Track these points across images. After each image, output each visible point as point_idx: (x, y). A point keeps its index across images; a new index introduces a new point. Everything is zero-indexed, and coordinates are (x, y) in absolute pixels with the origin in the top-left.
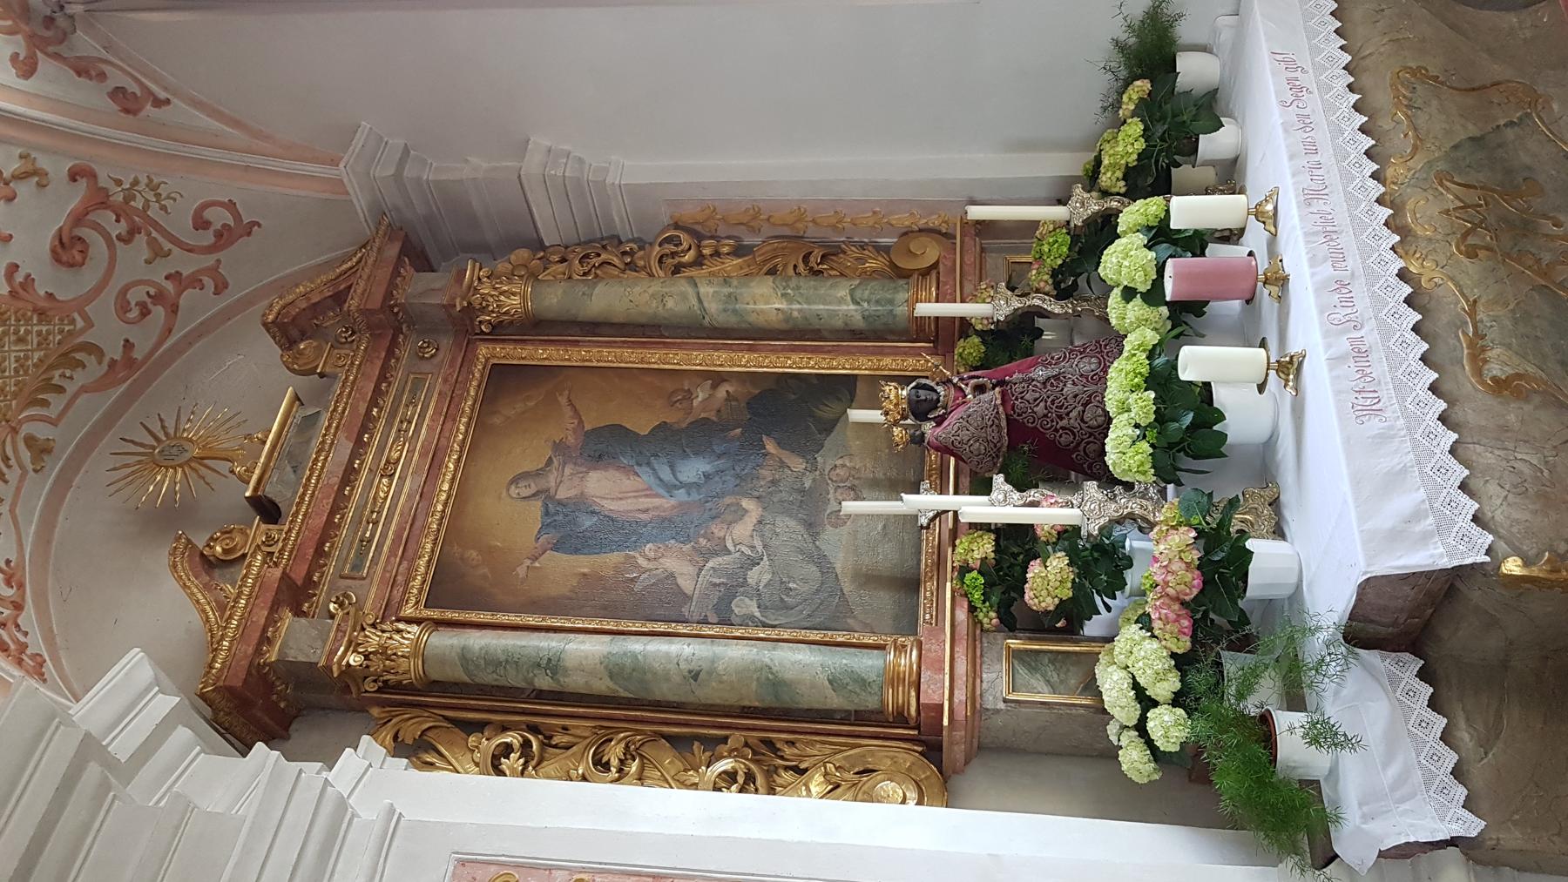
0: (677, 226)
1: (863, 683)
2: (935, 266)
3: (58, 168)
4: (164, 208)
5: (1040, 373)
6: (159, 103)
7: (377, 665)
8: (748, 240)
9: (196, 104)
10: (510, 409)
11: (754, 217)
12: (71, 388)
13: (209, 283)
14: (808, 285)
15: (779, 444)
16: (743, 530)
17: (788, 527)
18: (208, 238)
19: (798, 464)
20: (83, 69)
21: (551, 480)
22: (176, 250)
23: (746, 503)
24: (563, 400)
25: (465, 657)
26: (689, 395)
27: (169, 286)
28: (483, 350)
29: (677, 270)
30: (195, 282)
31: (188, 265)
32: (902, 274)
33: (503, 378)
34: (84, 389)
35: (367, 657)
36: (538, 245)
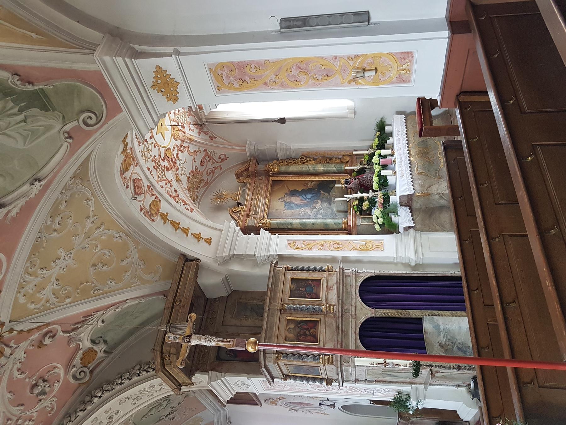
0: (303, 155)
1: (339, 224)
2: (348, 161)
3: (202, 149)
4: (215, 155)
5: (364, 176)
6: (215, 138)
7: (263, 225)
8: (315, 158)
9: (220, 137)
10: (276, 188)
11: (316, 154)
12: (200, 187)
13: (219, 168)
14: (327, 165)
15: (323, 191)
16: (318, 205)
17: (326, 204)
19: (327, 194)
20: (206, 133)
22: (216, 163)
23: (318, 201)
24: (286, 186)
25: (277, 223)
26: (307, 184)
27: (214, 169)
28: (271, 178)
29: (303, 163)
30: (217, 168)
31: (217, 165)
32: (343, 163)
33: (274, 182)
34: (201, 187)
35: (262, 224)
36: (278, 160)
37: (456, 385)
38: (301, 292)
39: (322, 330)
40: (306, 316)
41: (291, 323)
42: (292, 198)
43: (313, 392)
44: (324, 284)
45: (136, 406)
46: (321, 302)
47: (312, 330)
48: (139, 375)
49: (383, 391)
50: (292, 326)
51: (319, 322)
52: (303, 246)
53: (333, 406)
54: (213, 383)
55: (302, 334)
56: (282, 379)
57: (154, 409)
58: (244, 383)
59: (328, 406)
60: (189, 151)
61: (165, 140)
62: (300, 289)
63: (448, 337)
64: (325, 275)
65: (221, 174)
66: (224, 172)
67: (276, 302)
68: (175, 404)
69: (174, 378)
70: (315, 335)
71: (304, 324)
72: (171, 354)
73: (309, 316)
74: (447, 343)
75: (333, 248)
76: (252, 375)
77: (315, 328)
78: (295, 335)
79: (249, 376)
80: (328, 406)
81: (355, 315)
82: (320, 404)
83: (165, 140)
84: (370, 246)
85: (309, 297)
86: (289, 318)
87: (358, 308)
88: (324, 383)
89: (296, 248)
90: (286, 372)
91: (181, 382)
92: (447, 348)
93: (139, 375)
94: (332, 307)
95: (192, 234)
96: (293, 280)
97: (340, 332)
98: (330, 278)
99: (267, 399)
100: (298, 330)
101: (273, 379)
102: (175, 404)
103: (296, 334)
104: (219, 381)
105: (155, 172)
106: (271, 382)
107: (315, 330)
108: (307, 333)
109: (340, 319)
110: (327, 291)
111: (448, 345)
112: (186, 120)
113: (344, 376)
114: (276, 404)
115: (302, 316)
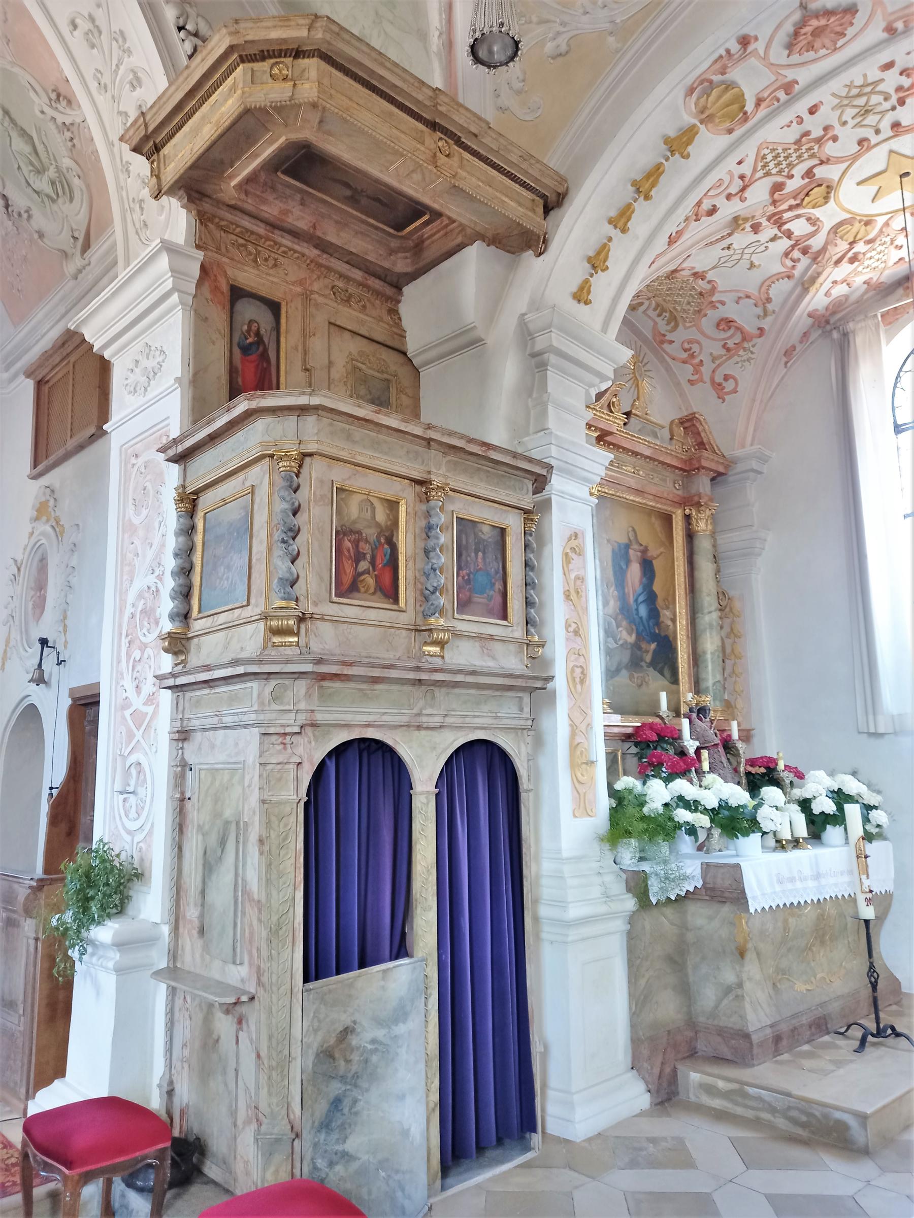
3: (766, 324)
4: (737, 363)
6: (786, 363)
10: (657, 524)
12: (658, 320)
13: (695, 377)
15: (654, 651)
16: (624, 634)
18: (719, 378)
20: (806, 335)
21: (635, 546)
22: (714, 366)
23: (634, 636)
24: (662, 550)
26: (667, 608)
27: (697, 361)
28: (679, 512)
30: (696, 371)
31: (706, 370)
33: (667, 519)
34: (656, 323)
37: (171, 1083)
38: (473, 555)
39: (372, 615)
40: (410, 564)
41: (388, 515)
42: (638, 565)
43: (123, 602)
44: (493, 627)
45: (65, 29)
46: (450, 613)
47: (370, 581)
48: (180, 29)
49: (132, 826)
50: (381, 516)
51: (395, 607)
52: (573, 576)
53: (40, 679)
54: (164, 261)
55: (357, 546)
56: (184, 487)
57: (27, 149)
58: (152, 374)
59: (40, 665)
60: (778, 277)
61: (859, 184)
62: (480, 554)
63: (374, 1058)
64: (518, 632)
65: (678, 384)
66: (682, 394)
67: (448, 471)
68: (39, 221)
69: (189, 116)
70: (358, 590)
71: (388, 557)
72: (295, 85)
73: (410, 573)
74: (355, 1057)
75: (571, 664)
76: (189, 395)
77: (379, 593)
78: (354, 522)
79: (186, 381)
80: (40, 665)
81: (419, 727)
82: (44, 642)
83: (859, 184)
84: (582, 775)
85: (460, 578)
86: (402, 509)
87: (436, 737)
88: (167, 626)
89: (567, 554)
90: (207, 501)
91: (166, 150)
92: (337, 1055)
93: (180, 29)
94: (435, 649)
95: (610, 239)
96: (503, 531)
97: (376, 673)
98: (512, 647)
99: (53, 491)
100: (371, 533)
101: (182, 458)
102: (39, 221)
103: (359, 526)
104: (169, 284)
105: (791, 135)
106: (171, 453)
107: (372, 590)
108: (364, 565)
109: (411, 675)
110: (480, 637)
111: (348, 1061)
112: (865, 270)
113: (207, 691)
114: (37, 519)
115: (410, 553)
